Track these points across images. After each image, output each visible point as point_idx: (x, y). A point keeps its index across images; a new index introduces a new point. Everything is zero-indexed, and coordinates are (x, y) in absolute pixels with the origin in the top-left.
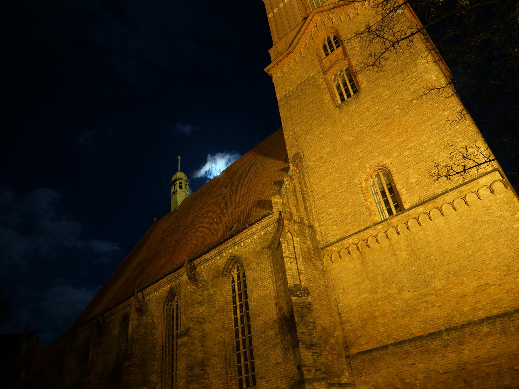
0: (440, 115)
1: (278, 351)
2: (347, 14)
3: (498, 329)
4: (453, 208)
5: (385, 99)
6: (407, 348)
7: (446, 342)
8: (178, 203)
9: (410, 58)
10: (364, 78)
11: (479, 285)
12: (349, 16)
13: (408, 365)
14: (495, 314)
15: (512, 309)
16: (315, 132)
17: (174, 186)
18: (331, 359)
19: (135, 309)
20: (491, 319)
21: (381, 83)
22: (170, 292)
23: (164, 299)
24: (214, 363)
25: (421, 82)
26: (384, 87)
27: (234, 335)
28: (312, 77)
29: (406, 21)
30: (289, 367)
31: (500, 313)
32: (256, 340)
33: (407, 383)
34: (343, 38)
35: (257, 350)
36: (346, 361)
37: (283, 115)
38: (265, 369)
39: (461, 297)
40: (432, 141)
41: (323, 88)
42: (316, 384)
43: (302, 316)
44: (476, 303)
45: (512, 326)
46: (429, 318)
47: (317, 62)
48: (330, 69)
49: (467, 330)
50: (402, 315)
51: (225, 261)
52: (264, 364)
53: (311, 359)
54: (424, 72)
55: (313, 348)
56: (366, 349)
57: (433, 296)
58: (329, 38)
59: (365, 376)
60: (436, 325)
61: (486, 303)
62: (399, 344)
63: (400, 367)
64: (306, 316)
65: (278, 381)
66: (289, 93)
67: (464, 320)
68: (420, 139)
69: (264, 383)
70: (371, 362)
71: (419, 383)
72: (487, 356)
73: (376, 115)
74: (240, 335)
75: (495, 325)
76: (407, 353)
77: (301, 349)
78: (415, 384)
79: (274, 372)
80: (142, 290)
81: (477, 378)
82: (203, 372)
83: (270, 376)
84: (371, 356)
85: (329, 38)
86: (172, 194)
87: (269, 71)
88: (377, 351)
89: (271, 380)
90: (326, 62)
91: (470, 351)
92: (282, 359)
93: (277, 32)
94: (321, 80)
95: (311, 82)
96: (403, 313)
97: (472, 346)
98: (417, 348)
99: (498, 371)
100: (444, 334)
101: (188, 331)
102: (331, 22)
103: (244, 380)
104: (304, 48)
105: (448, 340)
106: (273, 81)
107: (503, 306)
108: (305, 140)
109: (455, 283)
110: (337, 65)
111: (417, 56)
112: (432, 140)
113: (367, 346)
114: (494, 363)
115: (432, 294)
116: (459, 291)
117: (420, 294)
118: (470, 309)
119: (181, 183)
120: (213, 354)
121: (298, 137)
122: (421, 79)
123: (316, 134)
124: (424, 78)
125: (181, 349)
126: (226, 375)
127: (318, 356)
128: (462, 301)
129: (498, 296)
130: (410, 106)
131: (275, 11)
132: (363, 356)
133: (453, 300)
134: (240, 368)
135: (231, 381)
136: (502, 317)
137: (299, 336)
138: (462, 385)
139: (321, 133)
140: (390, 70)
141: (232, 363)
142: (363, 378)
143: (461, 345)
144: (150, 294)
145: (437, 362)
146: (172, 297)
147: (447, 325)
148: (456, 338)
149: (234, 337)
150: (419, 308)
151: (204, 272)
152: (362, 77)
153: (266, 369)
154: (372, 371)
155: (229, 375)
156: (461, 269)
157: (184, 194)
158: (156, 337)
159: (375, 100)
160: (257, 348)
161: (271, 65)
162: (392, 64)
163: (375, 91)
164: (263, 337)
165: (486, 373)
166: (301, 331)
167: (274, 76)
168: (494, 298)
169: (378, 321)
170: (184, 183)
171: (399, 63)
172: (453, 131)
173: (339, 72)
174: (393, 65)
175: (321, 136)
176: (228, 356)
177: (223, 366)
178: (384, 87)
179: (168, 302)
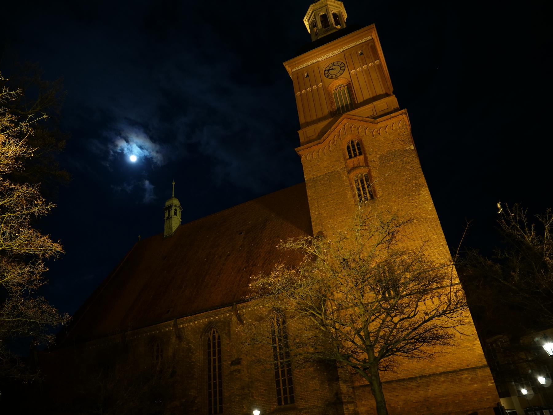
0: (431, 236)
1: (316, 382)
2: (371, 130)
3: (450, 379)
4: (432, 302)
8: (173, 230)
9: (415, 187)
12: (372, 132)
13: (394, 396)
14: (449, 371)
16: (338, 219)
17: (168, 211)
26: (394, 202)
28: (337, 171)
29: (415, 157)
30: (325, 393)
31: (451, 370)
32: (297, 372)
33: (392, 407)
34: (366, 149)
35: (298, 380)
38: (304, 393)
41: (346, 185)
42: (348, 405)
44: (439, 363)
45: (457, 379)
46: (410, 369)
48: (353, 171)
49: (432, 378)
51: (268, 310)
53: (346, 390)
54: (424, 201)
55: (347, 383)
61: (445, 363)
63: (389, 397)
65: (315, 401)
66: (316, 177)
67: (431, 372)
69: (304, 402)
72: (441, 394)
78: (398, 408)
82: (249, 392)
85: (352, 142)
89: (310, 401)
91: (432, 390)
93: (304, 113)
94: (345, 178)
95: (336, 176)
97: (434, 388)
98: (401, 386)
99: (447, 403)
100: (418, 379)
103: (283, 399)
104: (333, 143)
105: (420, 383)
107: (454, 367)
108: (329, 223)
114: (445, 398)
119: (176, 210)
120: (256, 379)
121: (322, 218)
122: (422, 206)
123: (338, 221)
125: (235, 374)
127: (349, 388)
129: (452, 360)
137: (339, 375)
139: (342, 221)
142: (363, 402)
143: (428, 386)
145: (412, 396)
147: (420, 374)
150: (404, 362)
151: (246, 315)
152: (379, 188)
155: (272, 395)
160: (298, 379)
162: (402, 187)
164: (303, 371)
166: (340, 371)
168: (449, 361)
170: (178, 210)
171: (407, 188)
175: (343, 223)
177: (266, 388)
178: (394, 202)
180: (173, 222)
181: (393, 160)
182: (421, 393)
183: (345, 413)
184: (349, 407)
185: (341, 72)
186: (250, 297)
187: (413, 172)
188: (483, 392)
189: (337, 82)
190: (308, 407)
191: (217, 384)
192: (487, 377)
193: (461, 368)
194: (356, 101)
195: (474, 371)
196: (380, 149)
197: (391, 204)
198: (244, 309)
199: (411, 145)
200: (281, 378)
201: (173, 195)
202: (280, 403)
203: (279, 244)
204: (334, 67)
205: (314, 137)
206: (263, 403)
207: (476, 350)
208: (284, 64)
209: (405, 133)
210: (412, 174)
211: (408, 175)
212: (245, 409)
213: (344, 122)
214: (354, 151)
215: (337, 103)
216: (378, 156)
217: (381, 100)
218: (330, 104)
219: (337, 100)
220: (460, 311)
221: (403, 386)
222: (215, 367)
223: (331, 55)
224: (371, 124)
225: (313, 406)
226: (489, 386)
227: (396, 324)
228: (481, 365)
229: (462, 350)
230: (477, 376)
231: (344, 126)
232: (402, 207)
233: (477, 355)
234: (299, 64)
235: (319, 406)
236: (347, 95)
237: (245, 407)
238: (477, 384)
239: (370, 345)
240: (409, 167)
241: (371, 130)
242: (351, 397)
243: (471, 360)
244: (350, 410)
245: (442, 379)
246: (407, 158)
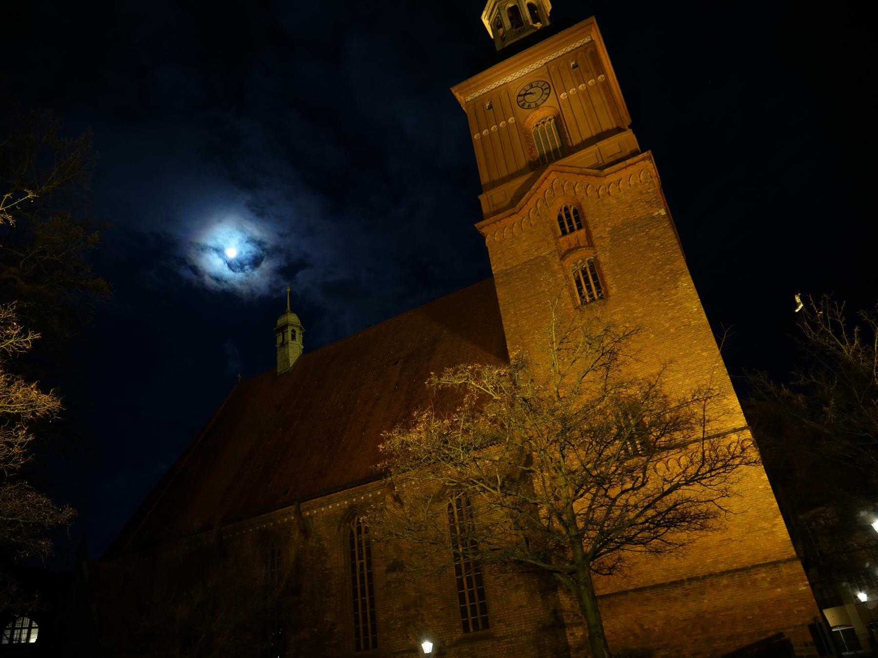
0: (698, 354)
1: (521, 593)
2: (595, 189)
3: (736, 582)
6: (648, 594)
8: (290, 362)
9: (669, 276)
10: (614, 282)
11: (722, 539)
12: (598, 191)
14: (734, 568)
20: (731, 572)
21: (634, 296)
22: (350, 509)
24: (431, 603)
25: (680, 309)
26: (637, 301)
27: (454, 572)
28: (544, 257)
30: (536, 611)
31: (739, 567)
33: (646, 629)
34: (589, 218)
37: (502, 298)
39: (704, 549)
40: (687, 381)
42: (574, 628)
44: (718, 556)
45: (749, 580)
48: (570, 255)
49: (708, 581)
50: (644, 561)
53: (569, 605)
54: (684, 298)
56: (603, 594)
60: (678, 574)
61: (727, 557)
63: (639, 613)
65: (522, 625)
68: (675, 375)
69: (503, 626)
72: (724, 606)
75: (734, 578)
78: (654, 630)
82: (416, 613)
85: (566, 209)
86: (280, 345)
87: (481, 229)
88: (616, 596)
90: (565, 242)
91: (709, 601)
92: (527, 602)
94: (556, 267)
100: (686, 583)
102: (573, 191)
106: (487, 245)
107: (742, 561)
108: (533, 340)
111: (678, 276)
112: (687, 381)
113: (605, 591)
114: (730, 612)
118: (712, 561)
119: (293, 331)
120: (427, 593)
121: (523, 333)
122: (681, 306)
129: (739, 552)
130: (666, 335)
131: (484, 133)
133: (697, 551)
143: (702, 594)
144: (312, 509)
146: (351, 517)
147: (689, 575)
148: (697, 588)
149: (455, 574)
153: (506, 612)
154: (610, 616)
155: (453, 617)
157: (298, 348)
159: (625, 315)
162: (649, 276)
163: (627, 303)
167: (488, 236)
168: (735, 553)
170: (298, 331)
171: (657, 278)
174: (650, 277)
177: (444, 606)
180: (291, 351)
183: (569, 641)
184: (575, 631)
185: (544, 97)
186: (383, 465)
187: (666, 252)
188: (792, 601)
189: (538, 114)
190: (510, 634)
191: (368, 602)
193: (754, 563)
194: (570, 143)
195: (775, 567)
196: (611, 218)
197: (633, 304)
198: (403, 482)
199: (661, 208)
200: (466, 590)
201: (289, 308)
202: (466, 629)
203: (429, 379)
205: (505, 204)
206: (441, 630)
207: (777, 534)
208: (453, 90)
209: (651, 190)
210: (664, 256)
211: (658, 257)
212: (411, 640)
213: (551, 177)
214: (570, 222)
215: (540, 147)
216: (608, 229)
217: (609, 139)
218: (529, 150)
219: (539, 143)
220: (724, 474)
221: (661, 594)
222: (362, 577)
223: (526, 71)
224: (595, 177)
225: (518, 631)
226: (800, 591)
227: (614, 500)
229: (755, 534)
230: (780, 575)
231: (552, 183)
232: (650, 308)
233: (779, 541)
234: (477, 88)
235: (529, 632)
237: (411, 638)
238: (780, 587)
239: (576, 536)
240: (659, 244)
241: (595, 189)
242: (577, 615)
243: (770, 550)
244: (577, 636)
245: (725, 582)
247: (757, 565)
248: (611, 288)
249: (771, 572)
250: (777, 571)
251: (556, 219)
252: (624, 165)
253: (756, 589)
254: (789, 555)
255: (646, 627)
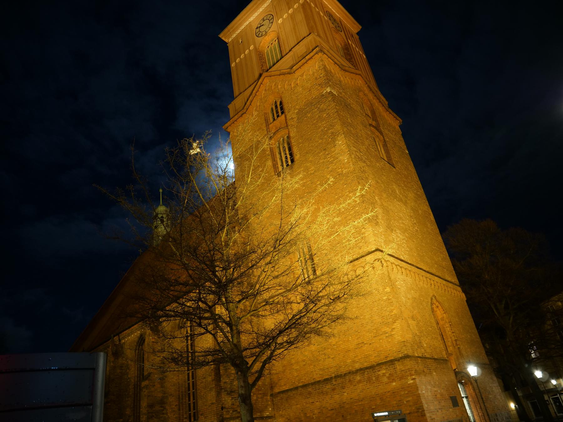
0: (347, 195)
1: (213, 394)
3: (366, 378)
5: (311, 174)
6: (310, 389)
7: (334, 386)
9: (331, 138)
10: (298, 150)
11: (358, 343)
14: (365, 366)
15: (376, 363)
18: (255, 398)
19: (111, 353)
20: (362, 370)
23: (135, 344)
26: (311, 162)
27: (187, 378)
31: (368, 366)
33: (308, 417)
34: (285, 106)
36: (271, 399)
39: (346, 352)
43: (226, 369)
44: (355, 357)
45: (374, 376)
47: (264, 127)
49: (347, 377)
50: (309, 363)
52: (204, 404)
53: (230, 403)
56: (284, 390)
57: (330, 350)
58: (276, 102)
59: (282, 411)
62: (305, 386)
63: (304, 404)
64: (229, 368)
67: (347, 370)
70: (287, 400)
71: (316, 417)
72: (357, 398)
73: (304, 188)
74: (191, 378)
75: (364, 375)
76: (310, 393)
77: (223, 395)
78: (313, 418)
79: (210, 410)
80: (118, 334)
81: (350, 414)
82: (162, 409)
83: (207, 413)
84: (287, 395)
85: (276, 102)
87: (227, 129)
90: (273, 126)
91: (348, 394)
96: (310, 362)
99: (363, 409)
100: (333, 380)
101: (149, 376)
103: (192, 415)
105: (335, 385)
107: (371, 361)
109: (344, 341)
110: (279, 133)
114: (361, 403)
115: (329, 348)
116: (346, 347)
117: (321, 347)
124: (339, 159)
126: (179, 411)
128: (346, 355)
132: (282, 395)
134: (189, 405)
135: (183, 416)
136: (369, 369)
138: (341, 419)
140: (317, 147)
141: (184, 401)
142: (281, 412)
143: (343, 389)
145: (327, 402)
147: (336, 373)
148: (340, 383)
149: (187, 380)
150: (320, 359)
156: (348, 330)
158: (129, 376)
161: (229, 123)
163: (305, 165)
165: (356, 411)
166: (224, 381)
168: (366, 354)
169: (293, 367)
172: (354, 212)
173: (282, 139)
176: (181, 396)
177: (177, 403)
179: (139, 346)
181: (310, 111)
182: (337, 397)
185: (270, 24)
188: (402, 393)
192: (407, 372)
195: (392, 365)
199: (327, 87)
204: (264, 23)
210: (328, 123)
213: (266, 82)
214: (277, 112)
216: (296, 111)
219: (269, 59)
226: (409, 384)
228: (400, 356)
229: (379, 338)
233: (396, 342)
234: (234, 31)
236: (278, 49)
243: (390, 350)
245: (358, 378)
246: (323, 104)
247: (380, 363)
248: (296, 155)
249: (389, 369)
250: (393, 368)
251: (269, 111)
252: (305, 61)
253: (379, 383)
254: (403, 354)
255: (308, 415)
